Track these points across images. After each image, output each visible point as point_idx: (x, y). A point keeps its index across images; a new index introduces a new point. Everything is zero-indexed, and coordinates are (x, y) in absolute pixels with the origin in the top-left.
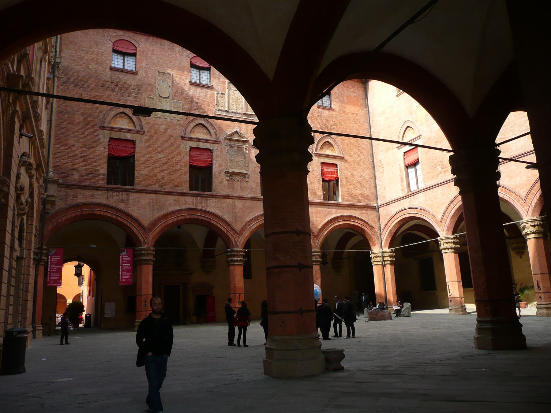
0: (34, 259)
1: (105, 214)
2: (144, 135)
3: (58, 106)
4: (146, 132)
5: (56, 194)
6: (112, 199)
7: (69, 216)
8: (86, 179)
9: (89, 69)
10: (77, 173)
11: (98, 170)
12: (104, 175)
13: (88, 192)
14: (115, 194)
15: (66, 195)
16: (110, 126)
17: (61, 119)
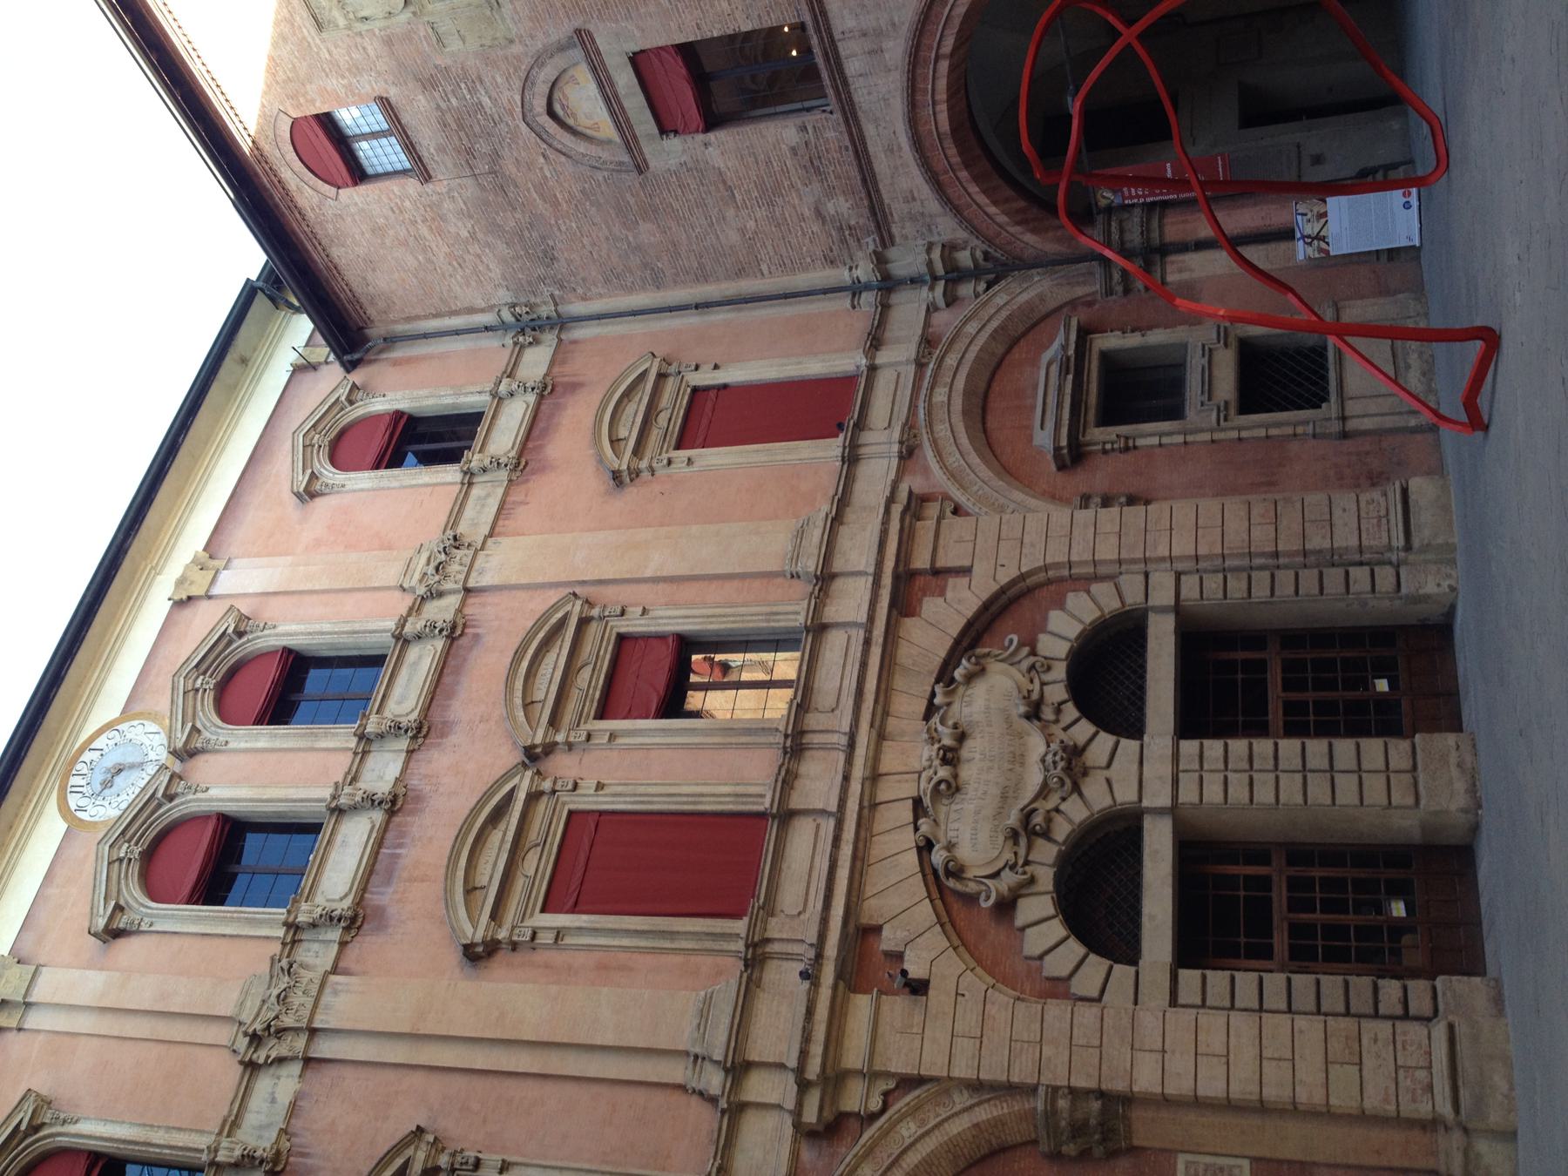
1: (942, 96)
2: (591, 27)
3: (643, 288)
4: (577, 24)
6: (879, 87)
8: (838, 177)
9: (473, 235)
10: (830, 206)
11: (794, 150)
12: (804, 129)
13: (881, 164)
15: (912, 218)
16: (616, 138)
17: (677, 274)
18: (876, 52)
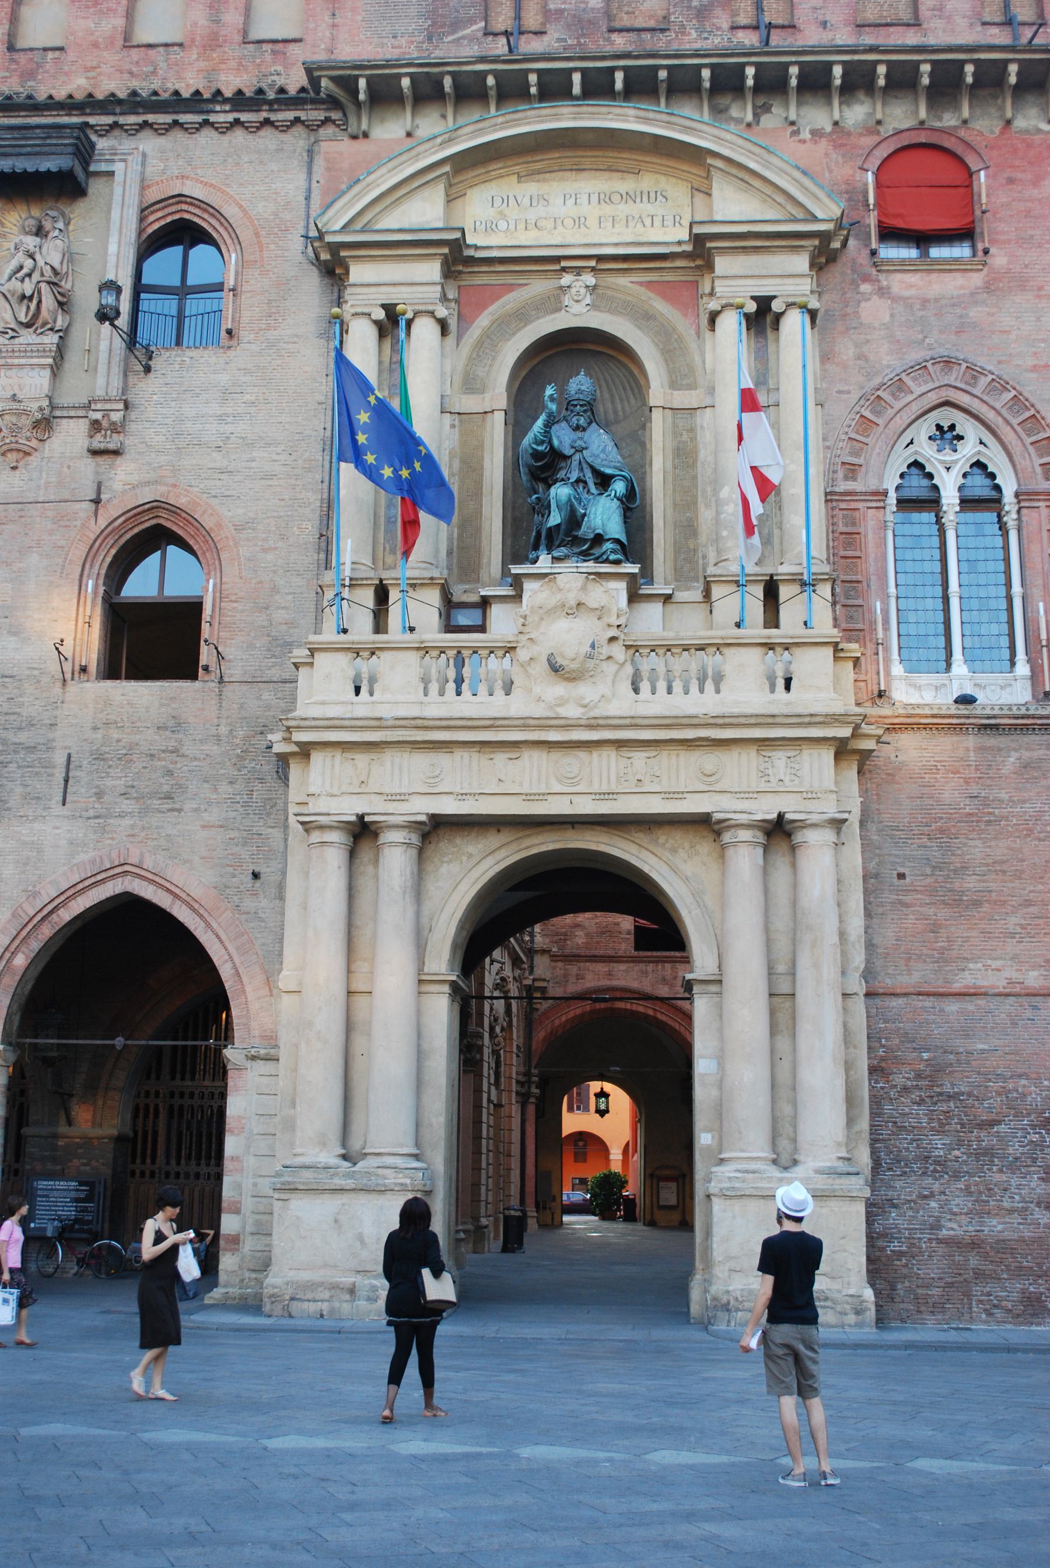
0: (517, 1093)
5: (548, 975)
7: (571, 1014)
8: (598, 942)
11: (618, 924)
12: (629, 933)
13: (602, 968)
14: (650, 967)
15: (566, 976)
18: (664, 980)
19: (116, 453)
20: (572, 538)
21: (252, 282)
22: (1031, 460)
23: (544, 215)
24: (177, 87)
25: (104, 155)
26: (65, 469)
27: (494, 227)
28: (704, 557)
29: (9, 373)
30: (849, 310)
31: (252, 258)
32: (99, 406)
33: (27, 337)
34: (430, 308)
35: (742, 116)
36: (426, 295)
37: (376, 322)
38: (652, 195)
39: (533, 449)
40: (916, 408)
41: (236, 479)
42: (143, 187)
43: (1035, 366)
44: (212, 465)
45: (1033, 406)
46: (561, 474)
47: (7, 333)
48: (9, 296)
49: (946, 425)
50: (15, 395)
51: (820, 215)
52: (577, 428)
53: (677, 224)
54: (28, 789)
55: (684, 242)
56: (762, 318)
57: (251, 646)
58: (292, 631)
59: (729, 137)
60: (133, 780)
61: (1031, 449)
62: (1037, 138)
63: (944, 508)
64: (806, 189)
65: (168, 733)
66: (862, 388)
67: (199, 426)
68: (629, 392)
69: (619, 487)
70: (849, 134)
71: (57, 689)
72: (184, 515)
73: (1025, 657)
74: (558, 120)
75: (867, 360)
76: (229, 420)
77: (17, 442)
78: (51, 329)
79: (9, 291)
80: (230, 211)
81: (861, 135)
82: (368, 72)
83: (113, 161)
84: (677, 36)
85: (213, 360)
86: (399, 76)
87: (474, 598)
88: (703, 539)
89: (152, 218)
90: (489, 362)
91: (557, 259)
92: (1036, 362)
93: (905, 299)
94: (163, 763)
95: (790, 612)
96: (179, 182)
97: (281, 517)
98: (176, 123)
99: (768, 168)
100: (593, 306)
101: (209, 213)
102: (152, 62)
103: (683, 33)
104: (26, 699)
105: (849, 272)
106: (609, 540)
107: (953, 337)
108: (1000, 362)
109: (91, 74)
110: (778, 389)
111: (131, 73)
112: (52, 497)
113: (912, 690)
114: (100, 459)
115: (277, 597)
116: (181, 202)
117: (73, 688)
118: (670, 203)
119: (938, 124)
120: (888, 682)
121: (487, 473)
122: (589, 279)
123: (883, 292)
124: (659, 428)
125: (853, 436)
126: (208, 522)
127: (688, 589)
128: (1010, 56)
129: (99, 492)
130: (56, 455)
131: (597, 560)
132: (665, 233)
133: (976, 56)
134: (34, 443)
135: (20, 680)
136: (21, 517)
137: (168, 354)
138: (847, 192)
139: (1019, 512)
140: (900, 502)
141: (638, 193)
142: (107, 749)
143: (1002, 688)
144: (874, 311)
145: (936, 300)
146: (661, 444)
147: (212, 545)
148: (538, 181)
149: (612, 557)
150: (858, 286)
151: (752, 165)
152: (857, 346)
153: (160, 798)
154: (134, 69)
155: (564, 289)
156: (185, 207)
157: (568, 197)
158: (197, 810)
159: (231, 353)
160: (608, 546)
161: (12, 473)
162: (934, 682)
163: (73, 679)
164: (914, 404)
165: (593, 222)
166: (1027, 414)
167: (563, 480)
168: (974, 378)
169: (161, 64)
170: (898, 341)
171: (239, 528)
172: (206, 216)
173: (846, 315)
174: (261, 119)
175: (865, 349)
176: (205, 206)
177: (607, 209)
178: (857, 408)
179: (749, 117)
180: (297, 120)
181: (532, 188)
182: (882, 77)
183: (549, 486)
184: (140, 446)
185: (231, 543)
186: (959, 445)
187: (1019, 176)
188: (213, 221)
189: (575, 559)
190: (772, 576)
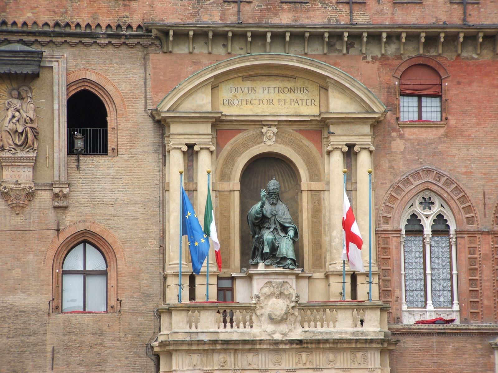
19: (66, 208)
20: (273, 256)
21: (122, 124)
22: (462, 216)
23: (254, 98)
24: (78, 21)
25: (47, 58)
26: (42, 215)
27: (232, 103)
28: (325, 258)
29: (13, 169)
30: (387, 145)
31: (121, 112)
32: (57, 186)
33: (21, 153)
34: (208, 146)
35: (341, 48)
36: (205, 140)
37: (184, 153)
38: (302, 89)
39: (256, 216)
40: (414, 192)
41: (121, 220)
42: (68, 74)
43: (466, 172)
44: (110, 213)
45: (464, 191)
46: (266, 225)
47: (11, 150)
48: (10, 132)
49: (427, 197)
50: (17, 181)
51: (376, 110)
52: (273, 204)
53: (313, 104)
54: (35, 363)
55: (317, 116)
56: (350, 154)
57: (132, 297)
58: (150, 290)
59: (337, 72)
60: (83, 358)
61: (462, 210)
62: (471, 62)
63: (425, 236)
64: (370, 98)
65: (97, 336)
66: (391, 182)
67: (103, 195)
68: (291, 178)
69: (291, 233)
70: (388, 59)
71: (46, 317)
72: (98, 236)
73: (457, 302)
74: (262, 60)
75: (394, 169)
76: (116, 191)
77: (19, 203)
78: (32, 149)
79: (10, 129)
80: (109, 88)
81: (394, 59)
82: (174, 28)
83: (52, 61)
84: (312, 6)
85: (107, 162)
86: (189, 30)
87: (228, 276)
88: (324, 250)
89: (71, 89)
90: (231, 167)
91: (261, 121)
92: (465, 170)
93: (410, 140)
94: (96, 350)
95: (362, 290)
96: (83, 72)
97: (142, 238)
98: (80, 42)
99: (354, 87)
100: (276, 142)
101: (98, 87)
102: (64, 6)
103: (315, 5)
104: (31, 322)
105: (387, 127)
106: (289, 259)
107: (431, 158)
108: (450, 170)
109: (35, 11)
110: (356, 183)
111: (54, 12)
112: (37, 228)
113: (410, 316)
114: (57, 210)
115: (142, 275)
116: (85, 81)
117: (54, 317)
118: (309, 92)
119: (428, 54)
120: (401, 314)
121: (232, 219)
122: (275, 130)
123: (401, 137)
124: (305, 200)
125: (388, 204)
126: (110, 241)
127: (318, 272)
128: (460, 30)
129: (58, 225)
130: (37, 208)
131: (283, 267)
132: (308, 109)
133: (445, 30)
134: (26, 202)
135: (28, 313)
136: (23, 237)
137: (85, 159)
138: (387, 88)
139: (456, 238)
140: (406, 231)
141: (296, 88)
142: (70, 344)
143: (447, 315)
144: (398, 145)
145: (424, 141)
146: (307, 207)
147: (112, 250)
148: (251, 81)
149: (291, 267)
150: (391, 134)
151: (347, 85)
152: (390, 162)
153: (95, 366)
154: (56, 10)
155: (263, 134)
156: (87, 84)
157: (264, 89)
158: (112, 370)
159: (115, 159)
160: (289, 262)
161: (16, 216)
162: (420, 313)
163: (52, 312)
164: (413, 190)
165: (275, 101)
166: (461, 195)
167: (267, 228)
168: (439, 177)
169: (69, 8)
170: (408, 160)
171: (124, 243)
172: (97, 89)
173: (385, 147)
174: (122, 42)
175: (393, 163)
176: (97, 84)
177: (283, 96)
178: (389, 192)
179: (345, 51)
180: (139, 43)
181: (248, 84)
182: (404, 38)
183: (260, 229)
184: (76, 204)
185: (121, 250)
186: (432, 206)
187: (463, 80)
188: (100, 92)
189: (274, 266)
190: (354, 272)
